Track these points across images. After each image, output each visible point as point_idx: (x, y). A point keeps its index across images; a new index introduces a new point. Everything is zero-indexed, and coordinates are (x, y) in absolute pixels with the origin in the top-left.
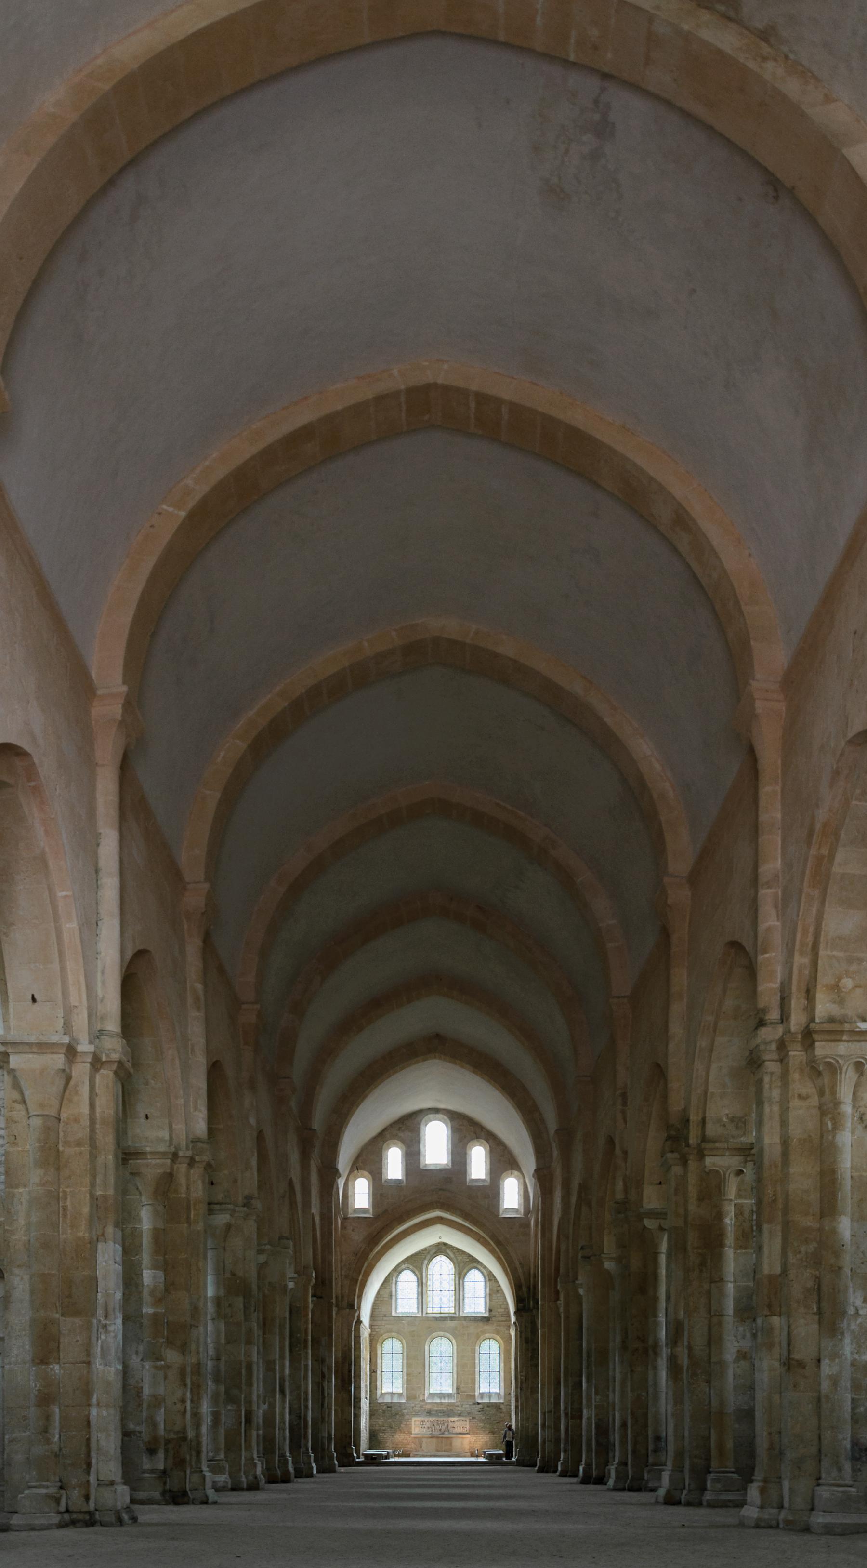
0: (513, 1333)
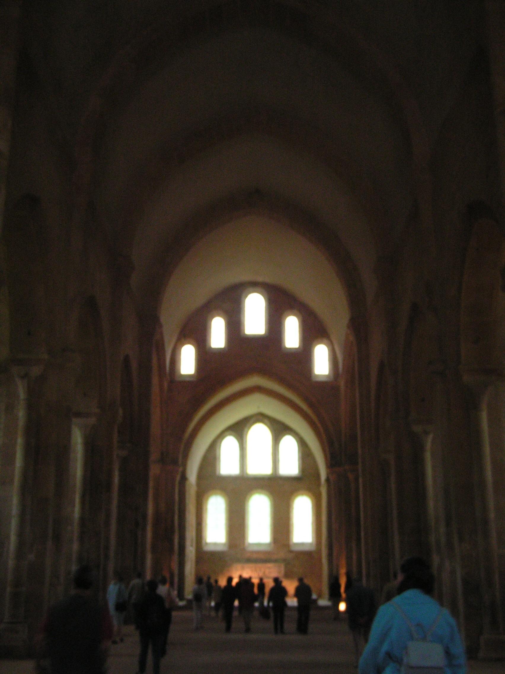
0: (324, 491)
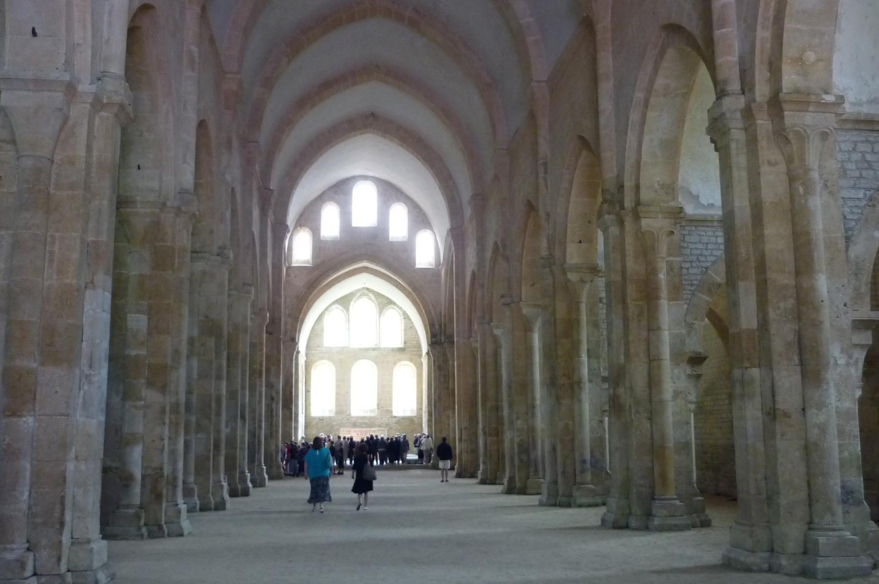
0: (425, 361)
